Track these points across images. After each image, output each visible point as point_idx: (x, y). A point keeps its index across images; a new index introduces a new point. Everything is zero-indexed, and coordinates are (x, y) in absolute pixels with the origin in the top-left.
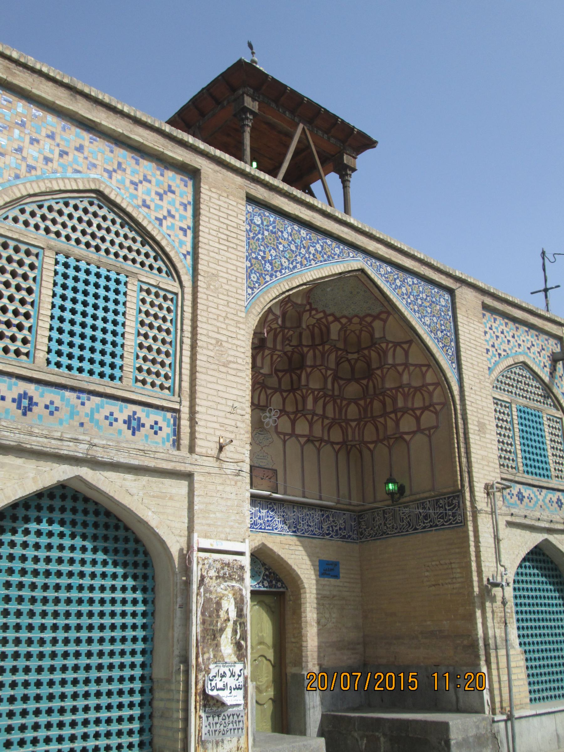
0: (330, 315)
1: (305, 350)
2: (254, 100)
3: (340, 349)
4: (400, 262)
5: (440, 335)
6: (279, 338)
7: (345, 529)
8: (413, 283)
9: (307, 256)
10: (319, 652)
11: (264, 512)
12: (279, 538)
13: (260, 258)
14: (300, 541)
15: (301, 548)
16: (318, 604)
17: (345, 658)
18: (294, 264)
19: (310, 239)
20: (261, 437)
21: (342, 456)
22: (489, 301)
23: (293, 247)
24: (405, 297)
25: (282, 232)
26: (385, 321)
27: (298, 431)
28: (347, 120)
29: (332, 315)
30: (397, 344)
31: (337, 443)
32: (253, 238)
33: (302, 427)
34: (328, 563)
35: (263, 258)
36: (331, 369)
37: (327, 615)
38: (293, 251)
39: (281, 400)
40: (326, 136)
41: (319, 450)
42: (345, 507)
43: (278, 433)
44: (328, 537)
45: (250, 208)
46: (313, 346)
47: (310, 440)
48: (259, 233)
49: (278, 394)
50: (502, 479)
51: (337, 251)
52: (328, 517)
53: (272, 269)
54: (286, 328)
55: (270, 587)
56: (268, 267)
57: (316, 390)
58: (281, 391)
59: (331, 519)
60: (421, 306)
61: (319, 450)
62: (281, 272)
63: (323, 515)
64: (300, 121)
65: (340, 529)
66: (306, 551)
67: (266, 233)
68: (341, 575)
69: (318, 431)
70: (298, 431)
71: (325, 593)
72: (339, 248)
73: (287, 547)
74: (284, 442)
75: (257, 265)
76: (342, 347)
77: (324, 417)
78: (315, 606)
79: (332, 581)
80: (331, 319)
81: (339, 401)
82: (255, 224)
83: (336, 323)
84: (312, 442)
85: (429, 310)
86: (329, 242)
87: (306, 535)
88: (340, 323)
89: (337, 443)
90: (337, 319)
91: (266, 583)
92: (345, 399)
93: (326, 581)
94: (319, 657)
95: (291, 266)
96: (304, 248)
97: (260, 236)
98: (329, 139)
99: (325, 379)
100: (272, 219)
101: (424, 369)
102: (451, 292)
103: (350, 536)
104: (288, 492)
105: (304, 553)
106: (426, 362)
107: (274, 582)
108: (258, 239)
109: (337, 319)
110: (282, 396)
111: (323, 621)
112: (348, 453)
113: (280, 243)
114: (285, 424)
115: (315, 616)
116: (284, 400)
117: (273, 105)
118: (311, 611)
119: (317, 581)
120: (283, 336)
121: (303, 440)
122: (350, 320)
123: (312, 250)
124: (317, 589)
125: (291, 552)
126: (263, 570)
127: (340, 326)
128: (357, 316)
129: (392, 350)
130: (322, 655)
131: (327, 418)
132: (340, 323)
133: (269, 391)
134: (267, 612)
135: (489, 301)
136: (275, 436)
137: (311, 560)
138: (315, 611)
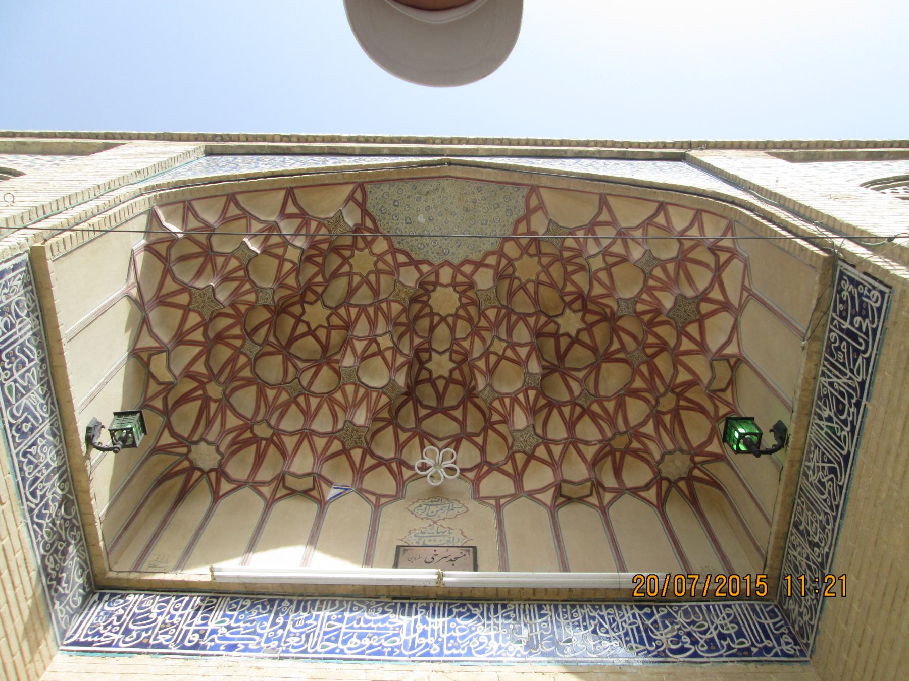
0: (462, 264)
7: (740, 634)
21: (677, 510)
26: (541, 207)
29: (467, 261)
31: (647, 487)
44: (680, 657)
49: (465, 443)
54: (381, 301)
57: (518, 392)
59: (681, 619)
63: (650, 616)
77: (573, 441)
81: (596, 407)
83: (482, 270)
84: (581, 500)
89: (647, 487)
90: (479, 265)
92: (608, 398)
101: (660, 220)
103: (768, 650)
109: (479, 265)
110: (475, 444)
112: (693, 501)
116: (483, 450)
122: (501, 253)
127: (491, 272)
132: (488, 266)
136: (473, 505)
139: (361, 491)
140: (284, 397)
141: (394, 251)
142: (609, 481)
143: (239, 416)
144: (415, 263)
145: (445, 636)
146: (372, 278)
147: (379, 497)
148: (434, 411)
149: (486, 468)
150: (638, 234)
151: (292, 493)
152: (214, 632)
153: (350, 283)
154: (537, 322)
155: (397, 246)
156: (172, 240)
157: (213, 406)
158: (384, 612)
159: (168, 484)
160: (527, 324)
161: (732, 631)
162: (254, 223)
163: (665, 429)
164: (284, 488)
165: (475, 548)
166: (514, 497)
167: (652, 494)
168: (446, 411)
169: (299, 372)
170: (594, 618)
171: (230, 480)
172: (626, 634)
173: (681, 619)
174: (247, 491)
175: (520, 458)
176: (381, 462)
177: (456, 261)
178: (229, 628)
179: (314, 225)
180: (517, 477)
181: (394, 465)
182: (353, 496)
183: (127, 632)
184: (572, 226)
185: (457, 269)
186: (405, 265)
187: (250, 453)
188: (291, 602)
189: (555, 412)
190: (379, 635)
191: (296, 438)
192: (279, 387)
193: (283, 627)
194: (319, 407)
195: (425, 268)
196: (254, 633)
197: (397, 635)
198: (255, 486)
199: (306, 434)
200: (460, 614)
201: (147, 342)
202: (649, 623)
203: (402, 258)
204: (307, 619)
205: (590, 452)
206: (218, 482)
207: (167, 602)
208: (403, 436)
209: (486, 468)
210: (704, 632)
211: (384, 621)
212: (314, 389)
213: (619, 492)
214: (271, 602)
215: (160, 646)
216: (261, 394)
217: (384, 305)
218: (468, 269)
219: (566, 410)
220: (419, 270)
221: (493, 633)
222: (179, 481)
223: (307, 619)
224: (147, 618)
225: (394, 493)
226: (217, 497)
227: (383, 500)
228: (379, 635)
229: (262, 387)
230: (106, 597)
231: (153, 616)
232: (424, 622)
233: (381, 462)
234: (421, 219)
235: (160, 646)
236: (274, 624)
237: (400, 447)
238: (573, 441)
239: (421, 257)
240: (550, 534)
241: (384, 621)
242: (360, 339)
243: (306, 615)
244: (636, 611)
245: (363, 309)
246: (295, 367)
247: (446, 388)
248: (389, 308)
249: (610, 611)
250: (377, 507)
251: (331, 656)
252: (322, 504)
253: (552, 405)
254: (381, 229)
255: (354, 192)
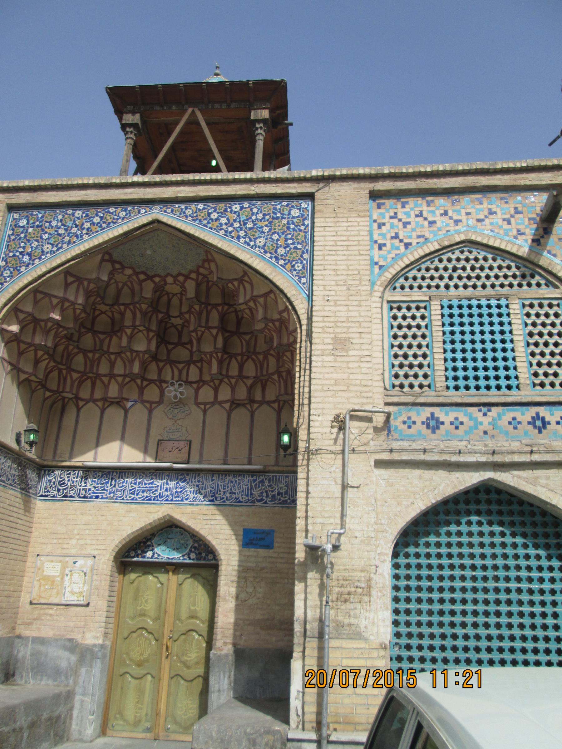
1: (187, 316)
2: (134, 113)
3: (219, 305)
4: (214, 194)
5: (281, 251)
6: (138, 315)
7: (286, 493)
8: (242, 208)
9: (79, 233)
10: (235, 630)
11: (172, 484)
12: (190, 509)
13: (18, 254)
14: (219, 510)
15: (220, 517)
16: (239, 577)
17: (274, 639)
18: (60, 245)
19: (87, 215)
20: (176, 411)
22: (381, 186)
23: (61, 231)
24: (224, 227)
25: (50, 222)
26: (214, 260)
27: (220, 398)
28: (236, 79)
29: (180, 274)
30: (241, 280)
31: (274, 402)
32: (14, 240)
33: (225, 394)
34: (255, 532)
35: (21, 253)
36: (213, 328)
37: (250, 590)
38: (60, 235)
39: (198, 371)
40: (224, 106)
41: (252, 414)
42: (285, 469)
43: (197, 404)
44: (259, 504)
45: (16, 216)
46: (189, 312)
47: (235, 404)
48: (22, 233)
50: (387, 404)
51: (123, 214)
52: (262, 482)
53: (30, 259)
55: (198, 559)
56: (26, 259)
58: (194, 362)
59: (266, 483)
60: (250, 229)
61: (252, 414)
62: (40, 258)
63: (254, 481)
64: (189, 107)
65: (279, 494)
66: (227, 520)
67: (30, 230)
68: (276, 545)
69: (242, 393)
70: (220, 398)
71: (249, 564)
72: (125, 211)
73: (202, 517)
74: (205, 411)
75: (13, 262)
76: (219, 301)
78: (235, 579)
79: (262, 552)
80: (181, 279)
81: (253, 357)
82: (20, 227)
83: (189, 280)
84: (244, 405)
85: (266, 229)
86: (112, 210)
87: (228, 503)
88: (154, 282)
89: (274, 402)
91: (193, 556)
92: (260, 353)
93: (252, 551)
94: (235, 636)
95: (55, 249)
96: (77, 226)
97: (22, 235)
98: (229, 106)
99: (215, 338)
100: (40, 216)
101: (272, 295)
102: (310, 196)
104: (253, 461)
105: (226, 523)
106: (268, 290)
107: (203, 555)
108: (20, 238)
109: (187, 277)
111: (243, 596)
113: (46, 233)
114: (206, 393)
115: (233, 590)
116: (201, 370)
117: (157, 108)
118: (226, 585)
119: (240, 552)
120: (141, 311)
121: (227, 406)
122: (198, 273)
123: (87, 225)
124: (240, 561)
125: (205, 522)
126: (191, 543)
128: (199, 267)
129: (241, 287)
130: (238, 633)
131: (247, 378)
133: (181, 366)
134: (204, 585)
135: (381, 186)
136: (194, 408)
137: (233, 530)
138: (235, 585)
139: (143, 402)
140: (97, 355)
141: (137, 274)
142: (258, 397)
143: (78, 372)
144: (150, 278)
145: (174, 491)
146: (129, 284)
147: (151, 403)
148: (176, 345)
149: (201, 384)
150: (261, 300)
151: (112, 403)
152: (90, 490)
153: (117, 287)
154: (223, 309)
155: (138, 270)
156: (15, 335)
157: (64, 372)
158: (152, 479)
159: (55, 405)
160: (218, 311)
161: (283, 491)
162: (53, 299)
163: (283, 379)
164: (107, 402)
165: (190, 441)
166: (213, 404)
167: (276, 405)
168: (183, 345)
169: (102, 342)
170: (232, 482)
171: (82, 400)
172: (243, 491)
173: (266, 483)
174: (91, 404)
175: (217, 382)
176: (151, 381)
177: (175, 273)
178: (95, 487)
179: (86, 283)
180: (216, 390)
181: (158, 383)
182: (139, 405)
183: (59, 490)
184: (231, 277)
185: (175, 278)
186: (145, 280)
187: (89, 383)
188: (117, 473)
189: (233, 359)
190: (150, 491)
191: (107, 378)
192: (94, 351)
193: (115, 486)
194: (116, 359)
195: (157, 279)
196: (104, 490)
197: (156, 490)
198: (95, 401)
199: (112, 376)
200: (181, 479)
201: (23, 377)
202: (253, 485)
203: (142, 277)
204: (123, 482)
205: (249, 382)
206: (77, 402)
207: (70, 474)
208: (161, 364)
209: (201, 384)
210: (272, 491)
211: (152, 483)
212: (111, 350)
213: (261, 403)
214: (109, 473)
215: (71, 497)
216: (85, 356)
217: (137, 305)
218: (181, 279)
219: (239, 358)
220: (154, 282)
221: (192, 490)
222: (60, 403)
223: (123, 482)
224: (64, 483)
225: (158, 400)
226: (79, 409)
227: (154, 405)
228: (150, 491)
229: (85, 352)
230: (47, 472)
231: (66, 482)
232: (167, 484)
233: (151, 381)
234: (149, 252)
235: (71, 497)
236: (111, 485)
237: (160, 371)
238: (241, 377)
239: (154, 273)
240: (224, 431)
241: (152, 483)
242: (128, 327)
243: (122, 480)
244: (250, 478)
245: (126, 305)
246: (99, 338)
247: (182, 328)
248: (141, 307)
249: (240, 478)
250: (150, 411)
251: (133, 501)
252: (126, 411)
253: (232, 356)
254: (126, 265)
255: (103, 257)
